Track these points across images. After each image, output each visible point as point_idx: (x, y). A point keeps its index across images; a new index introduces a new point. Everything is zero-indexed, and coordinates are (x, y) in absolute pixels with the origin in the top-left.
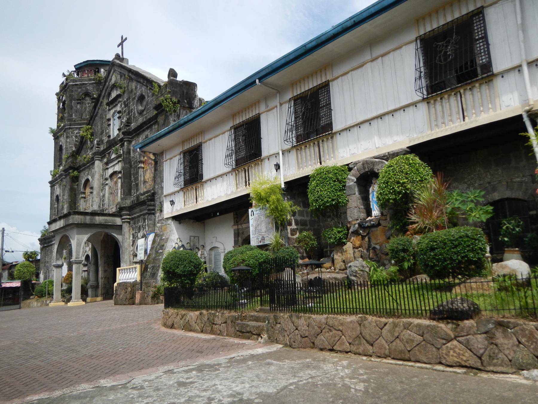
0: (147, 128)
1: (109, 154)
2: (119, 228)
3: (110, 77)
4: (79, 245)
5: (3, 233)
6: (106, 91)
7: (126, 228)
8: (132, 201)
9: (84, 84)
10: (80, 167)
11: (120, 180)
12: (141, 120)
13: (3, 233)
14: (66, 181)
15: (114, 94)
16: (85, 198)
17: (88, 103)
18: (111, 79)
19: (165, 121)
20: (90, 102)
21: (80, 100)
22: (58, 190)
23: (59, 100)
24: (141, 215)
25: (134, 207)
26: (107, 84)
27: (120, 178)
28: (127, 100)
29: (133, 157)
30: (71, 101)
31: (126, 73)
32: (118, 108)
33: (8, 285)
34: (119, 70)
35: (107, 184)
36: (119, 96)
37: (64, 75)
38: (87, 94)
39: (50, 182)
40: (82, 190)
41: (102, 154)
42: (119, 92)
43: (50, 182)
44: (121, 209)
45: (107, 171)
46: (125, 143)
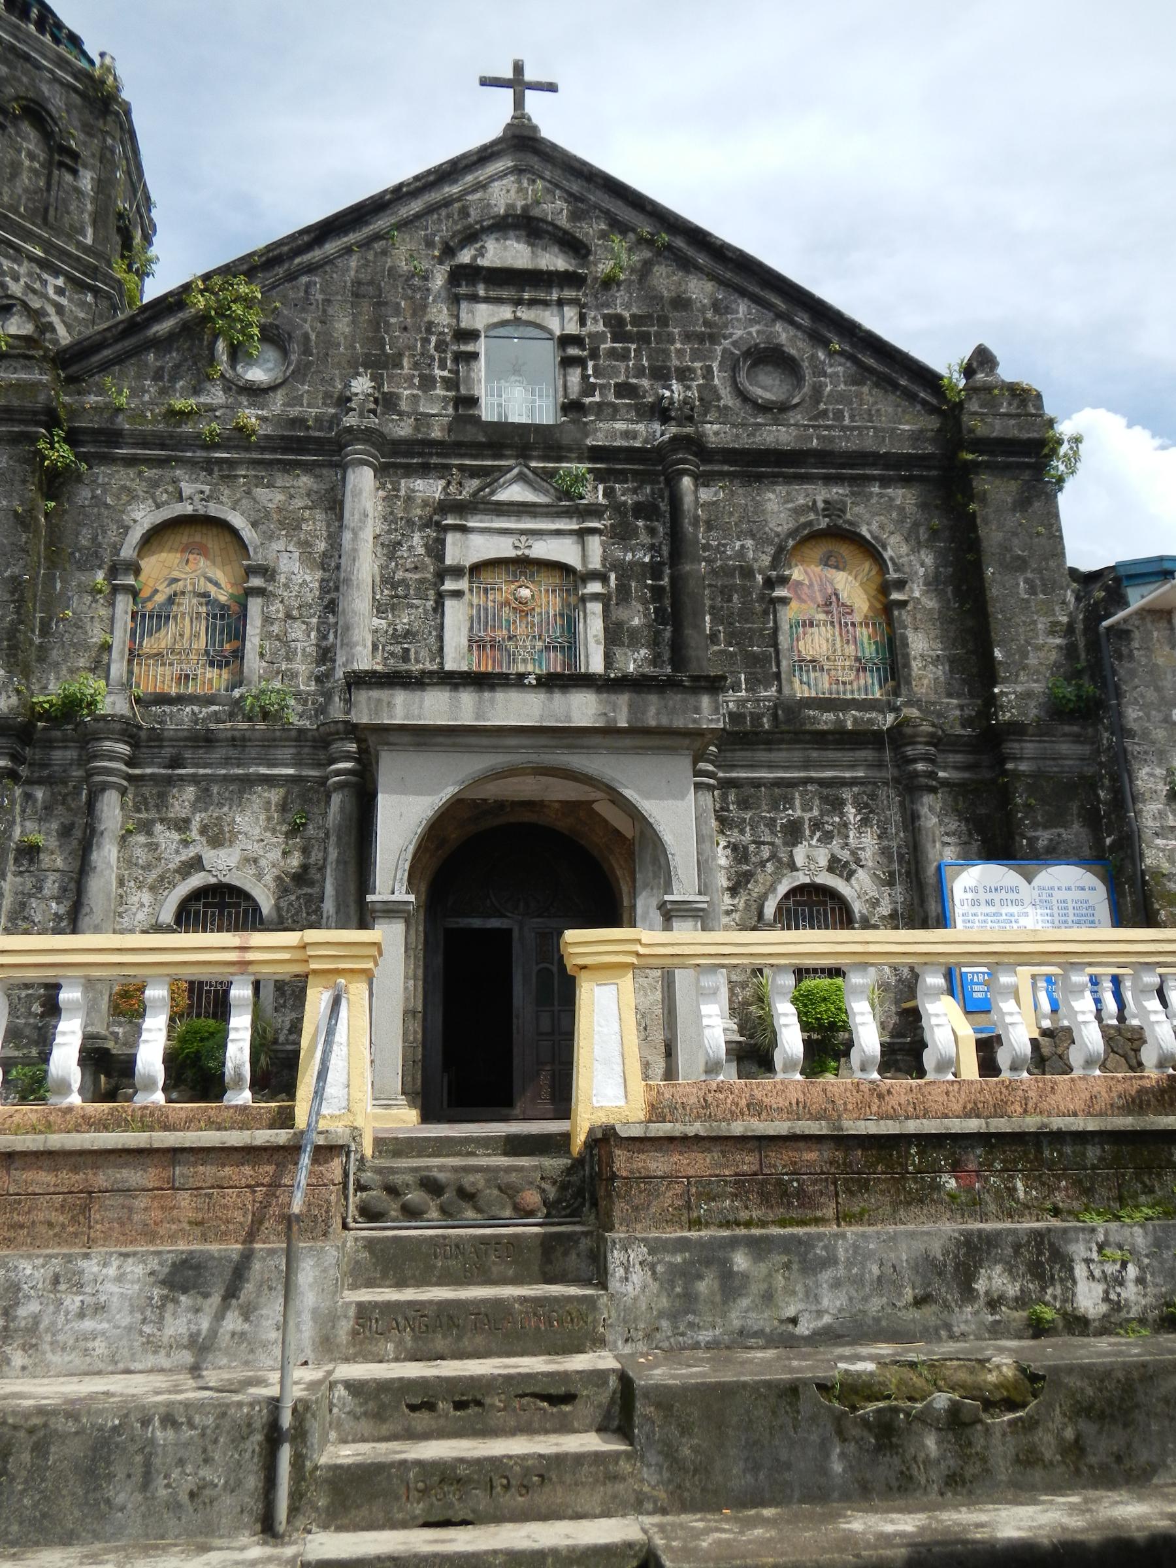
0: (828, 480)
1: (490, 476)
3: (483, 173)
6: (430, 210)
8: (735, 717)
9: (27, 58)
10: (113, 437)
11: (596, 608)
12: (778, 436)
15: (510, 253)
16: (134, 593)
17: (32, 156)
18: (482, 186)
19: (1023, 504)
20: (42, 156)
24: (806, 781)
25: (768, 742)
26: (455, 189)
27: (595, 597)
28: (636, 320)
29: (707, 547)
31: (646, 228)
32: (561, 322)
34: (575, 187)
35: (458, 594)
38: (35, 113)
40: (127, 552)
41: (401, 458)
42: (555, 261)
45: (450, 538)
46: (687, 482)
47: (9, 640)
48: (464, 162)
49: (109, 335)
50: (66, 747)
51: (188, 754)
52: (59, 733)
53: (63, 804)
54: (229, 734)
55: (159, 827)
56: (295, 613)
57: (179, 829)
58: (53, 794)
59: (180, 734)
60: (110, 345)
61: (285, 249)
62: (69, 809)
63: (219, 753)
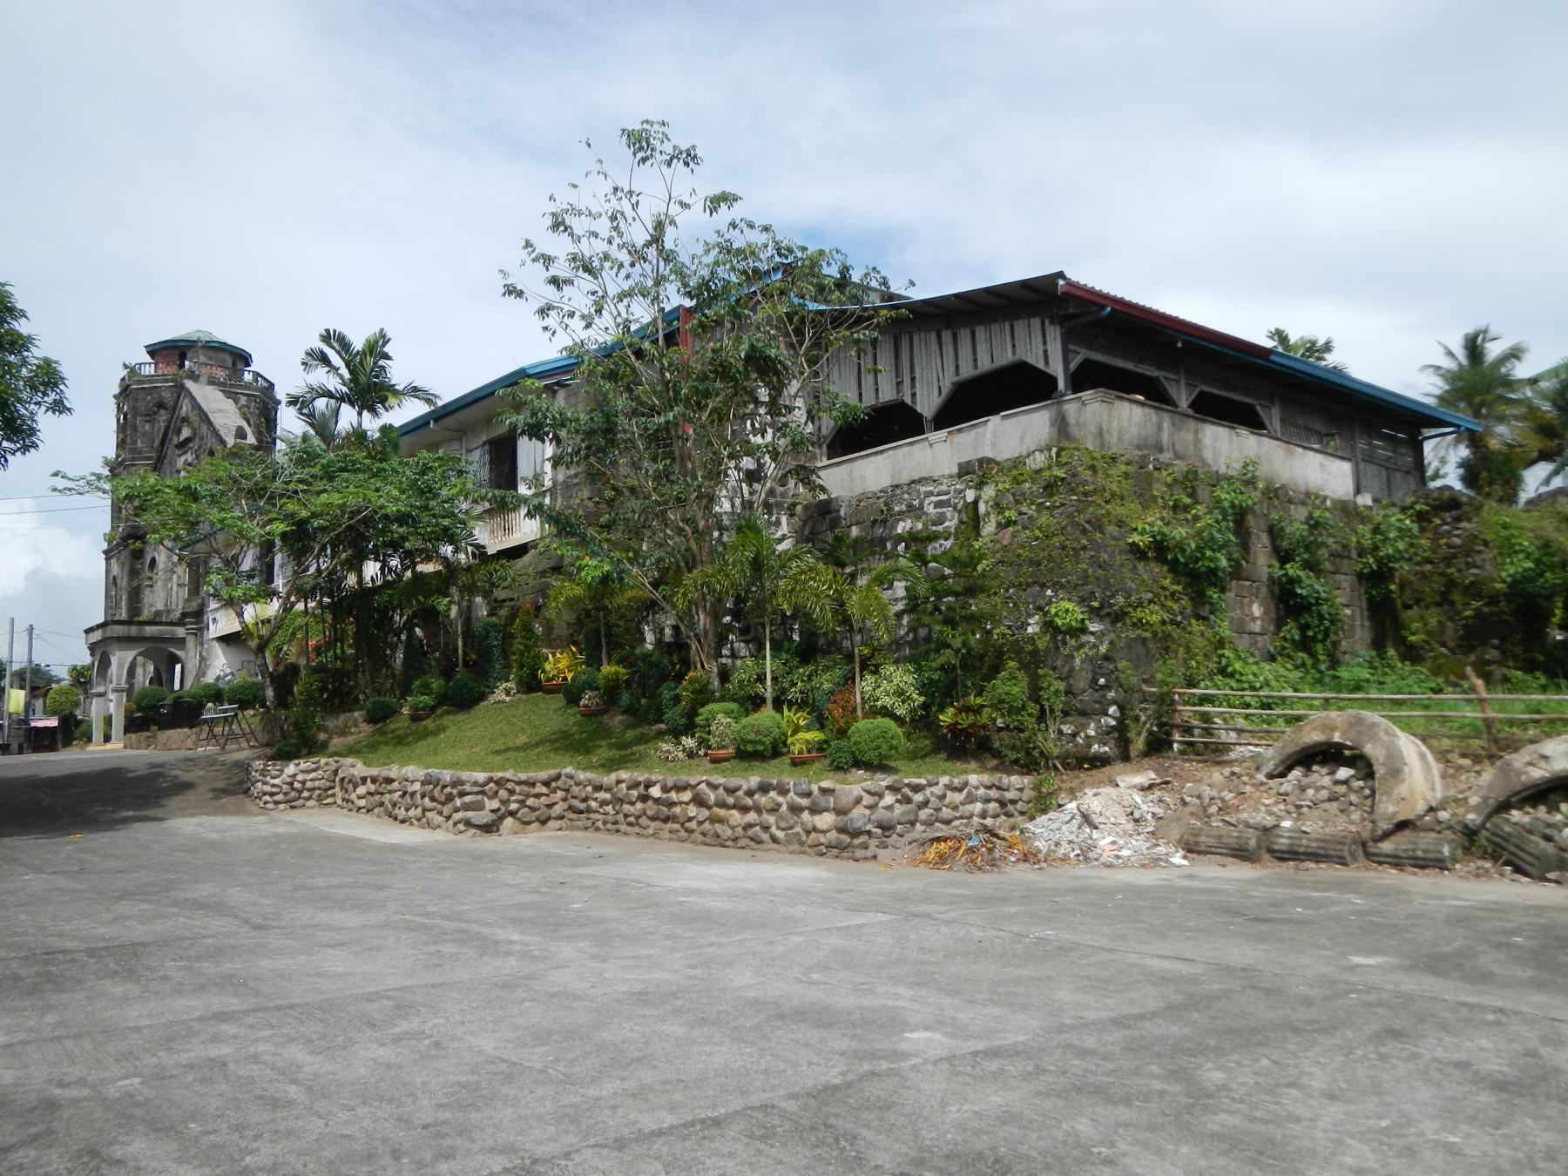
2: (181, 642)
4: (120, 666)
5: (31, 634)
7: (191, 642)
13: (31, 634)
14: (125, 554)
21: (150, 416)
22: (116, 570)
23: (119, 408)
30: (134, 417)
32: (189, 457)
33: (40, 724)
36: (188, 440)
37: (126, 366)
39: (105, 552)
43: (105, 552)
44: (184, 615)
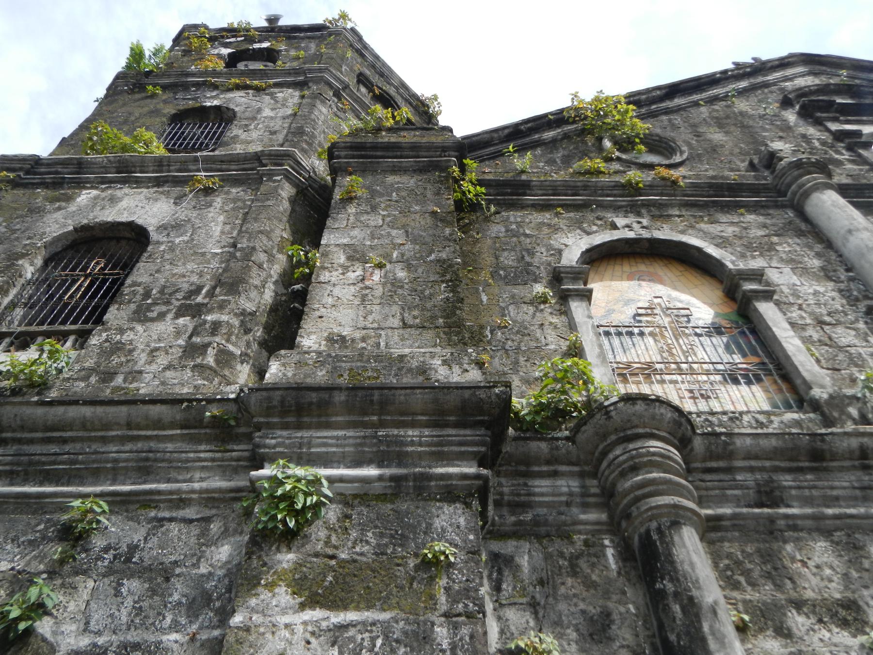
47: (447, 317)
48: (770, 65)
49: (496, 135)
50: (555, 474)
51: (787, 480)
52: (543, 445)
53: (574, 571)
54: (854, 443)
55: (798, 621)
56: (827, 319)
57: (844, 624)
58: (548, 557)
59: (764, 443)
60: (496, 144)
61: (644, 97)
62: (590, 585)
63: (844, 481)
